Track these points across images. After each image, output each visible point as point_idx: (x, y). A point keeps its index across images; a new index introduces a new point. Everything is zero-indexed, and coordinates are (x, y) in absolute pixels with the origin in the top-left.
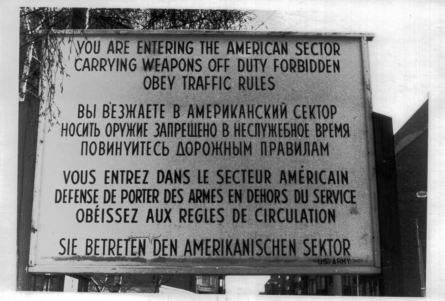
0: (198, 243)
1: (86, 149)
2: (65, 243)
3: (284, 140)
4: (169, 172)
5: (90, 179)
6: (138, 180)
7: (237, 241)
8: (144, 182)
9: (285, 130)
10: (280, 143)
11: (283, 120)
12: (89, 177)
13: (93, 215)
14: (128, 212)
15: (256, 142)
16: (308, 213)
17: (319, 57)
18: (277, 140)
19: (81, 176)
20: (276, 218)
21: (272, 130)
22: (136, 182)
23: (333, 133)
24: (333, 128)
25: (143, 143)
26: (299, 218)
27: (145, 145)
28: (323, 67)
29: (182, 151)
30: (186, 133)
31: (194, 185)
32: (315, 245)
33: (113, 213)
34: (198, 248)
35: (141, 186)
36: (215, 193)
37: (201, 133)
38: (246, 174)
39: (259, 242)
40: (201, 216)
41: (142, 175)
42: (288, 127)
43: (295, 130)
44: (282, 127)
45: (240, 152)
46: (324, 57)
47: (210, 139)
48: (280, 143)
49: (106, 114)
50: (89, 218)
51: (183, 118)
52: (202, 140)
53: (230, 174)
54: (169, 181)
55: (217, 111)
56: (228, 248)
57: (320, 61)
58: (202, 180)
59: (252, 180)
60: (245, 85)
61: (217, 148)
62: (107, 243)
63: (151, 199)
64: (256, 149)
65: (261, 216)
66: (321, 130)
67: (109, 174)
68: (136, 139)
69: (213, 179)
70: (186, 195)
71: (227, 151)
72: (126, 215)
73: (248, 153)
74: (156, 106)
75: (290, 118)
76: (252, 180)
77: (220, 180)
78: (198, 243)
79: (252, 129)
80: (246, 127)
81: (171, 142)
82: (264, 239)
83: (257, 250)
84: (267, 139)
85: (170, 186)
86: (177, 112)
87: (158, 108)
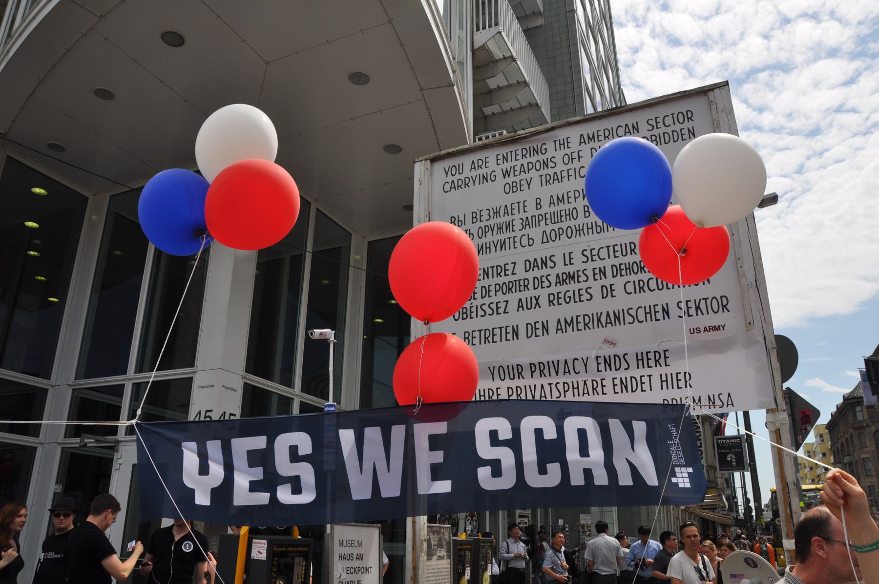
4: (535, 260)
6: (507, 273)
8: (513, 274)
17: (673, 128)
25: (509, 238)
27: (512, 240)
29: (547, 238)
30: (548, 222)
31: (560, 269)
38: (611, 249)
39: (630, 311)
41: (510, 267)
46: (677, 127)
47: (572, 223)
49: (475, 220)
51: (546, 209)
52: (564, 225)
53: (595, 252)
54: (536, 268)
55: (577, 195)
58: (567, 262)
61: (579, 230)
62: (483, 333)
68: (502, 237)
69: (578, 259)
70: (553, 279)
71: (590, 231)
76: (617, 254)
77: (585, 259)
81: (536, 233)
83: (629, 319)
85: (537, 273)
86: (538, 204)
87: (521, 205)
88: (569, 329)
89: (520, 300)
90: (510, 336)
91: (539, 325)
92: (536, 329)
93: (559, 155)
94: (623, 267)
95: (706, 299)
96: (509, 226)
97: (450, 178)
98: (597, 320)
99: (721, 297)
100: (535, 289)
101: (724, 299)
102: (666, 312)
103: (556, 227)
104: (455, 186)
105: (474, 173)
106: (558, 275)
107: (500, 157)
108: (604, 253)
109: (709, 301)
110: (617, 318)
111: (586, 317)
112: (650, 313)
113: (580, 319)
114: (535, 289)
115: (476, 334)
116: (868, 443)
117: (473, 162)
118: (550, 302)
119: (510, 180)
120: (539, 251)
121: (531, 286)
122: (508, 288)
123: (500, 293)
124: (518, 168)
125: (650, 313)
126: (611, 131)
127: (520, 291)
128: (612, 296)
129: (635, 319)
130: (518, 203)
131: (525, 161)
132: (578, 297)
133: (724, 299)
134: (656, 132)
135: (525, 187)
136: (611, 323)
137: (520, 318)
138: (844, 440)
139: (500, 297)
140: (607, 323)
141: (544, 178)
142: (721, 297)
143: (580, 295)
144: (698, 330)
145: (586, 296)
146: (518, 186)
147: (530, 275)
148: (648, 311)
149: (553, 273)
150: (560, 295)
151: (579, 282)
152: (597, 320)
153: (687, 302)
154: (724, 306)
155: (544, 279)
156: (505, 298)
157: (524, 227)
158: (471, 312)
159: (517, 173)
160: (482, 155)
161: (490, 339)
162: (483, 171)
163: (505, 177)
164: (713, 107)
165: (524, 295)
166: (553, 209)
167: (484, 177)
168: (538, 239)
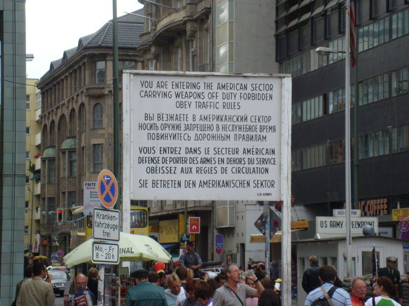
1: (150, 136)
2: (142, 182)
3: (245, 133)
4: (191, 148)
5: (153, 151)
6: (176, 152)
8: (179, 153)
9: (246, 128)
10: (244, 135)
11: (245, 123)
12: (152, 151)
13: (155, 170)
14: (171, 169)
15: (232, 134)
16: (256, 169)
18: (242, 133)
19: (148, 150)
20: (241, 171)
21: (240, 128)
22: (175, 153)
23: (268, 130)
24: (268, 127)
25: (178, 134)
26: (251, 172)
27: (179, 135)
28: (264, 97)
29: (197, 138)
31: (203, 155)
33: (164, 169)
35: (179, 156)
36: (212, 159)
37: (206, 129)
38: (227, 150)
40: (207, 171)
41: (178, 150)
42: (248, 127)
43: (250, 129)
44: (245, 127)
45: (224, 139)
46: (265, 92)
47: (210, 132)
48: (244, 135)
49: (159, 119)
50: (153, 171)
52: (206, 133)
56: (219, 184)
57: (263, 94)
59: (230, 153)
60: (226, 107)
63: (184, 162)
64: (232, 137)
65: (234, 170)
66: (262, 129)
67: (162, 149)
69: (212, 152)
70: (199, 160)
72: (171, 170)
73: (228, 139)
74: (184, 115)
75: (249, 123)
76: (230, 153)
79: (231, 127)
80: (227, 127)
81: (192, 134)
82: (235, 180)
83: (232, 185)
84: (238, 133)
85: (192, 155)
86: (194, 118)
88: (205, 186)
89: (182, 168)
90: (176, 186)
91: (191, 182)
93: (207, 92)
94: (232, 160)
95: (265, 181)
96: (178, 127)
97: (144, 89)
98: (218, 184)
100: (190, 163)
102: (248, 184)
103: (202, 133)
104: (147, 95)
105: (159, 90)
106: (202, 158)
107: (174, 84)
108: (224, 151)
109: (267, 182)
110: (227, 184)
112: (242, 183)
113: (211, 182)
114: (190, 163)
115: (159, 182)
116: (105, 121)
117: (158, 82)
118: (197, 171)
119: (180, 100)
120: (193, 144)
121: (188, 162)
122: (177, 161)
123: (172, 162)
124: (184, 94)
126: (233, 85)
127: (182, 163)
128: (226, 173)
129: (235, 185)
130: (184, 115)
131: (188, 91)
132: (210, 171)
134: (255, 92)
135: (187, 106)
137: (183, 178)
138: (67, 113)
139: (172, 165)
141: (198, 103)
143: (211, 170)
144: (261, 194)
145: (214, 171)
146: (184, 105)
147: (188, 156)
149: (199, 157)
150: (203, 169)
151: (211, 164)
152: (218, 184)
153: (258, 181)
155: (195, 159)
156: (175, 165)
157: (186, 129)
158: (156, 170)
159: (184, 97)
160: (164, 79)
161: (166, 185)
162: (164, 90)
163: (176, 97)
164: (283, 87)
165: (184, 166)
166: (202, 123)
167: (165, 94)
168: (193, 137)
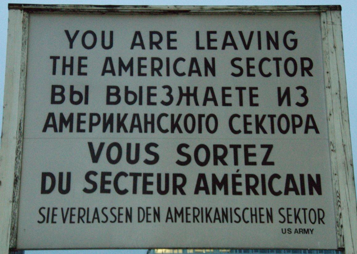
0: (179, 211)
7: (217, 210)
32: (290, 213)
34: (179, 216)
39: (238, 211)
78: (179, 211)
83: (235, 218)
88: (179, 219)
91: (151, 211)
92: (148, 214)
95: (305, 210)
99: (319, 210)
101: (321, 212)
102: (270, 216)
109: (307, 212)
110: (224, 216)
111: (196, 211)
112: (256, 215)
113: (190, 211)
125: (256, 215)
129: (241, 218)
133: (321, 212)
136: (219, 219)
140: (215, 219)
142: (319, 210)
148: (254, 213)
153: (288, 209)
154: (319, 219)
